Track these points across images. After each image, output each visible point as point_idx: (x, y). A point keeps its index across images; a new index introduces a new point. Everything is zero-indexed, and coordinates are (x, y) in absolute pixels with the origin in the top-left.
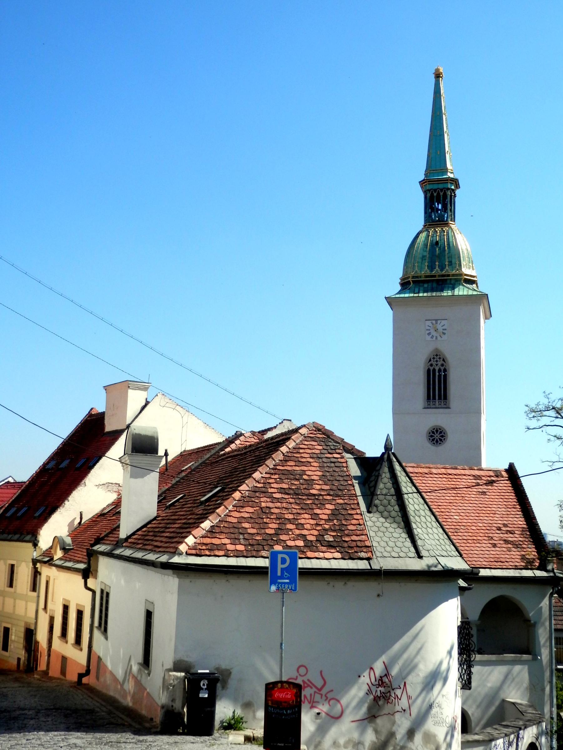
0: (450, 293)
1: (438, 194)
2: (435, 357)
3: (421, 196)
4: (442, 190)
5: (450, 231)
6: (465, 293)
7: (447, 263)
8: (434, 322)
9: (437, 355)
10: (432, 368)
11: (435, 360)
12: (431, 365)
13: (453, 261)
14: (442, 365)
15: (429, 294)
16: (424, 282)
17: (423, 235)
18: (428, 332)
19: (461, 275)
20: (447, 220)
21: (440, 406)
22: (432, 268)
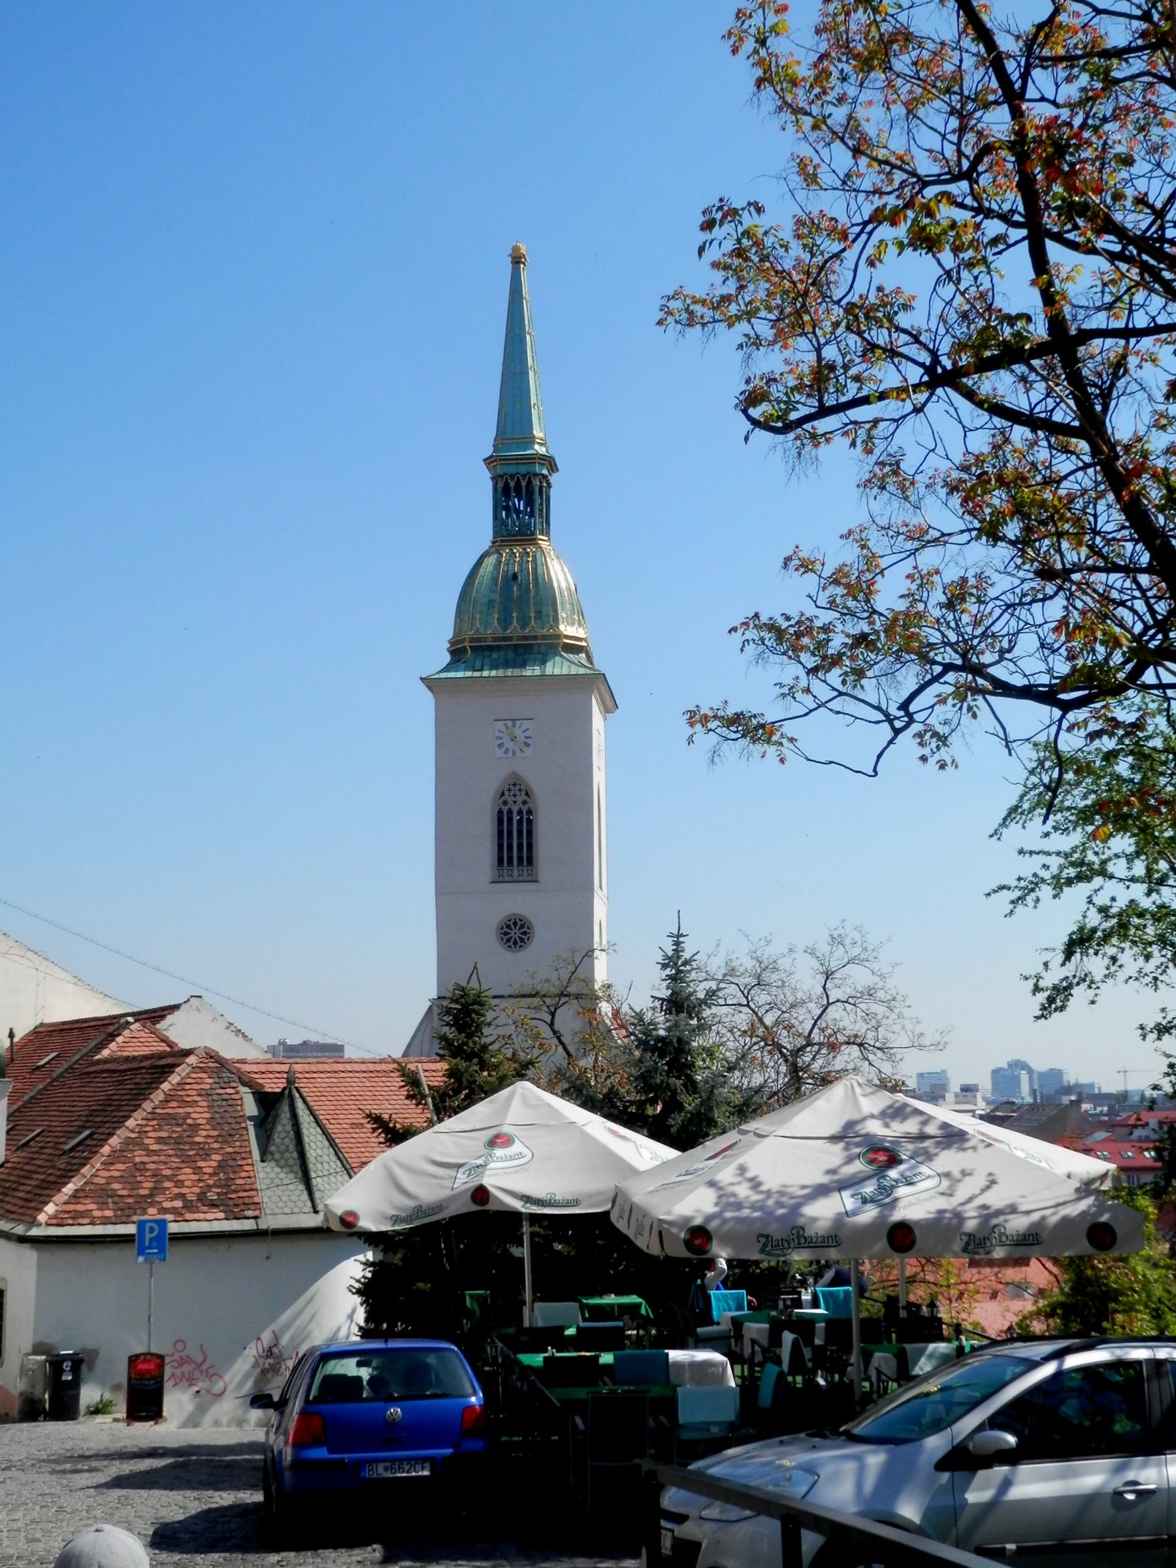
0: (537, 671)
1: (518, 483)
3: (490, 484)
4: (524, 476)
5: (538, 554)
6: (565, 671)
7: (532, 615)
8: (509, 723)
9: (515, 785)
10: (505, 809)
12: (505, 803)
13: (544, 610)
14: (525, 803)
15: (501, 673)
16: (491, 648)
17: (491, 561)
18: (499, 742)
19: (559, 636)
20: (533, 534)
21: (521, 878)
22: (505, 622)
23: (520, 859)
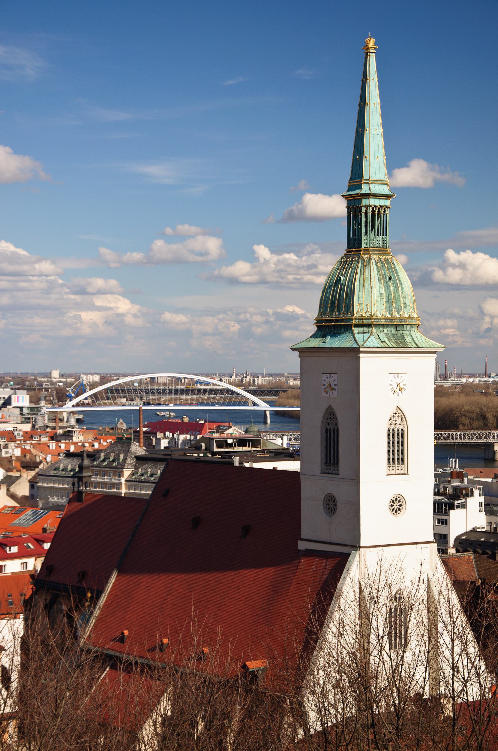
2: (395, 415)
11: (394, 419)
12: (391, 425)
14: (400, 425)
16: (383, 326)
21: (398, 472)
23: (398, 459)
